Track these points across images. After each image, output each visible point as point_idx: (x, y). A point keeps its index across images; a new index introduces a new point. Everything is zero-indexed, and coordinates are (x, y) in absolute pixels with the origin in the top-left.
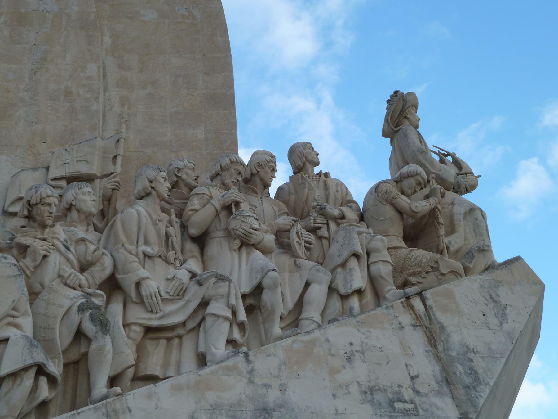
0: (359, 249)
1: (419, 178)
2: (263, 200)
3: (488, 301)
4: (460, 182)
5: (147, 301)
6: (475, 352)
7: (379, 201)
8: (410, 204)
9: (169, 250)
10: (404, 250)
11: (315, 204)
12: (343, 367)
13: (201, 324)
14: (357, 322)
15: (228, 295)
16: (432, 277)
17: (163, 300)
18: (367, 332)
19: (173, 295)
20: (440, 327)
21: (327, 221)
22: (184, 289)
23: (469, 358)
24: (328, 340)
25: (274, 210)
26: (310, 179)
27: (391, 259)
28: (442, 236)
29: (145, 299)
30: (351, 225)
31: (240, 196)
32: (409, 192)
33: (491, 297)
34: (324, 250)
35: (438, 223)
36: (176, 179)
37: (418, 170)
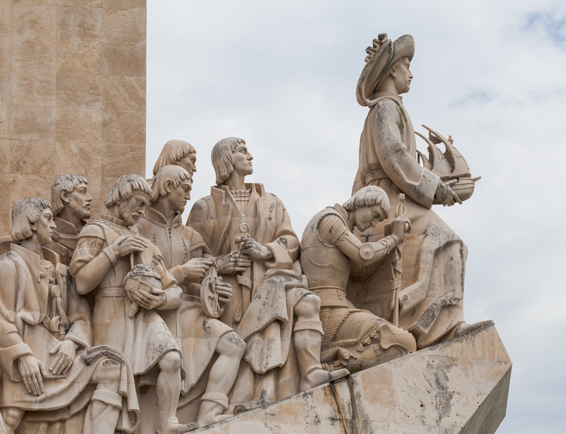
0: (284, 314)
1: (378, 209)
2: (172, 233)
3: (432, 387)
4: (445, 193)
5: (27, 382)
7: (319, 240)
8: (359, 249)
9: (53, 314)
10: (343, 312)
11: (239, 238)
13: (88, 407)
15: (119, 379)
16: (369, 353)
17: (45, 380)
18: (275, 427)
19: (56, 374)
20: (364, 421)
21: (252, 263)
22: (69, 366)
25: (185, 246)
26: (236, 197)
28: (396, 289)
29: (25, 379)
30: (279, 274)
31: (141, 244)
32: (363, 226)
33: (438, 382)
34: (243, 304)
35: (395, 270)
36: (63, 206)
37: (378, 197)
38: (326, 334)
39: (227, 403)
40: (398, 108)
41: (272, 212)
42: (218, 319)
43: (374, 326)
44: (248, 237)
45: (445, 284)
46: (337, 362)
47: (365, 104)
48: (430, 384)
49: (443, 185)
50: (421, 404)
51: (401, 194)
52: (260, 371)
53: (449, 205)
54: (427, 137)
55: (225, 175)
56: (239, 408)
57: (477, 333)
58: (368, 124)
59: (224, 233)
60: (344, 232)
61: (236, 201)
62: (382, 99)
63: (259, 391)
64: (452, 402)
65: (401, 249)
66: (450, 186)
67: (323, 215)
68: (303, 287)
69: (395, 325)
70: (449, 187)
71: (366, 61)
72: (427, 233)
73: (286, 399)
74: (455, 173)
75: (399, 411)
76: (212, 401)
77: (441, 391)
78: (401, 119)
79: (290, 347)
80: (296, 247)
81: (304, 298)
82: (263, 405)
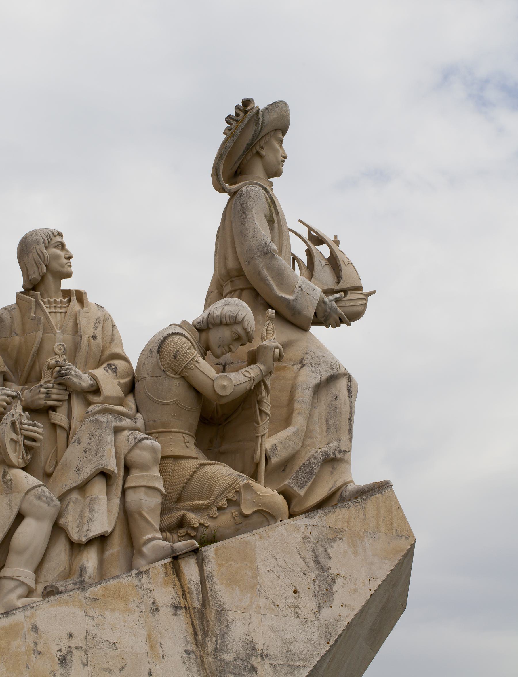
1: (239, 329)
3: (308, 567)
4: (328, 310)
6: (264, 656)
8: (214, 381)
10: (192, 464)
11: (53, 362)
12: (53, 673)
14: (86, 597)
18: (99, 615)
20: (217, 611)
21: (70, 396)
23: (252, 666)
24: (35, 628)
26: (50, 307)
27: (164, 485)
28: (262, 436)
30: (105, 411)
32: (218, 351)
33: (316, 560)
35: (260, 411)
37: (240, 314)
38: (168, 493)
39: (34, 582)
40: (267, 196)
41: (98, 329)
42: (23, 469)
43: (232, 484)
44: (65, 361)
45: (327, 431)
46: (182, 531)
47: (222, 190)
48: (307, 563)
49: (326, 299)
50: (294, 589)
51: (270, 310)
52: (78, 540)
53: (333, 327)
54: (306, 236)
55: (34, 278)
56: (50, 589)
57: (369, 497)
58: (227, 217)
59: (33, 355)
60: (193, 358)
61: (50, 313)
62: (245, 185)
63: (76, 567)
64: (335, 588)
65: (269, 383)
66: (336, 302)
67: (165, 335)
68: (138, 430)
69: (260, 483)
70: (334, 303)
71: (225, 133)
72: (305, 362)
73: (114, 578)
74: (342, 285)
75: (264, 599)
76: (13, 579)
77: (321, 573)
78: (271, 211)
79: (120, 509)
80: (128, 375)
81: (139, 444)
82: (82, 586)
